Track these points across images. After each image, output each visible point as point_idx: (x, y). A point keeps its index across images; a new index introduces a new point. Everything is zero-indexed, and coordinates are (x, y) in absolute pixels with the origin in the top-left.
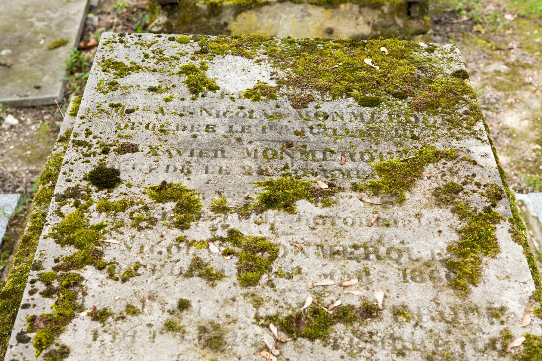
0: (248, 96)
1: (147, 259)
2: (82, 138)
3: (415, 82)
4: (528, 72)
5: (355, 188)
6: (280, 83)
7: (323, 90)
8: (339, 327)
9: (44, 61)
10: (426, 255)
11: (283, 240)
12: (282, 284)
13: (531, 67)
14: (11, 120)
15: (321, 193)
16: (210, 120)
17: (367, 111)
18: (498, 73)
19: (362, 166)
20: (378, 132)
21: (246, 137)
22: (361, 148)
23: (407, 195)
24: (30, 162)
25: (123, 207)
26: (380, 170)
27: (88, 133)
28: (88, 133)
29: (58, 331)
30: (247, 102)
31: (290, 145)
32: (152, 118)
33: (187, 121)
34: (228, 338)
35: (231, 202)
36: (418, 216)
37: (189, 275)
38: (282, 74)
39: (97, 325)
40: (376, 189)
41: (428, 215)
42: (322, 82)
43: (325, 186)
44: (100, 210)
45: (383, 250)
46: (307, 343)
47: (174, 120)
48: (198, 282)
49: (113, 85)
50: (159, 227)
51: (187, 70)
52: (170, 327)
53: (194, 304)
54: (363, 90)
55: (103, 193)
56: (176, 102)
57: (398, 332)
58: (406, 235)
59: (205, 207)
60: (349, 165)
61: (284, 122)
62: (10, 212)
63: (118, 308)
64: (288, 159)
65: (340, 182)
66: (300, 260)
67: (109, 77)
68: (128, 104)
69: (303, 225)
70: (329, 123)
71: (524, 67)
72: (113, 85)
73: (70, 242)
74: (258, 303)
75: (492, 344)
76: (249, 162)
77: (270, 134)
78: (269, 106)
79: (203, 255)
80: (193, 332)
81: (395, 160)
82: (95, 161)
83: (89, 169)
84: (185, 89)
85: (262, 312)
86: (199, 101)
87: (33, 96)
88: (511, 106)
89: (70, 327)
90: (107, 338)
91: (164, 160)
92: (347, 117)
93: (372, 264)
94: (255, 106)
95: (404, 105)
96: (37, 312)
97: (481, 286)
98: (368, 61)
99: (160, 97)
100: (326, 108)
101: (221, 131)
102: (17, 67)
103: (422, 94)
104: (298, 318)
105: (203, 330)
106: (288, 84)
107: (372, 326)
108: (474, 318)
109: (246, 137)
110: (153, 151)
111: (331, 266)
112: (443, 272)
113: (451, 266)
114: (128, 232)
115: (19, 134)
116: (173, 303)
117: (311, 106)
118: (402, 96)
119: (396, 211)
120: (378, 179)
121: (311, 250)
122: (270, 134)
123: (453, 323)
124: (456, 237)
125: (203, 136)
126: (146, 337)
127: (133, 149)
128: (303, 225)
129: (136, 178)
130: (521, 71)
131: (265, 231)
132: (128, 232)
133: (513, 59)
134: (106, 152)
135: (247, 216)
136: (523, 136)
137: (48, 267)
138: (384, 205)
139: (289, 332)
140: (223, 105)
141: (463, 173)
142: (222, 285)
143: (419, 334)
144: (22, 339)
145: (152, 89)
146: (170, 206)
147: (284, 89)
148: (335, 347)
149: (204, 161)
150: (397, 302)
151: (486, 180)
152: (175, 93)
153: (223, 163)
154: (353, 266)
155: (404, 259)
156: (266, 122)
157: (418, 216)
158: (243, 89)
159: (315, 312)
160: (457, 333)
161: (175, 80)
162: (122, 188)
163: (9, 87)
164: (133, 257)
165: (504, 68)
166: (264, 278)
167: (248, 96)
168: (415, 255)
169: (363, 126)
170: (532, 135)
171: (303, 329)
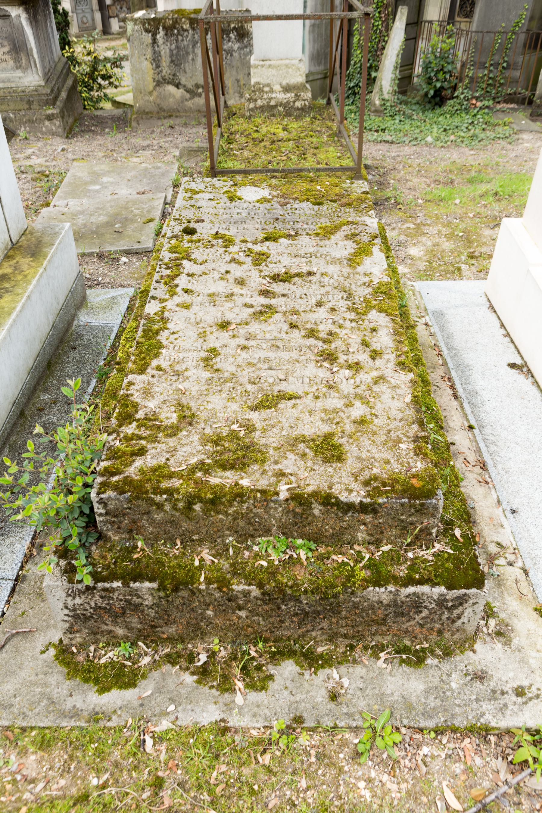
0: (258, 202)
1: (211, 257)
2: (178, 217)
3: (342, 196)
4: (427, 227)
5: (308, 234)
6: (274, 197)
7: (295, 199)
8: (297, 279)
9: (141, 229)
10: (338, 256)
11: (272, 252)
12: (271, 266)
13: (429, 225)
14: (124, 259)
15: (291, 236)
16: (239, 211)
17: (316, 207)
18: (409, 228)
19: (312, 227)
20: (321, 215)
21: (256, 217)
22: (312, 220)
23: (332, 236)
24: (137, 280)
25: (199, 241)
26: (320, 228)
27: (180, 216)
28: (180, 216)
29: (173, 280)
30: (258, 205)
31: (277, 219)
32: (211, 210)
33: (227, 211)
34: (248, 282)
35: (248, 239)
36: (336, 244)
37: (230, 262)
38: (275, 193)
39: (190, 278)
40: (317, 235)
41: (341, 244)
42: (295, 196)
43: (293, 234)
44: (188, 242)
45: (318, 255)
46: (282, 283)
47: (221, 211)
48: (233, 265)
49: (191, 198)
50: (216, 248)
51: (227, 192)
52: (222, 278)
53: (232, 272)
54: (316, 199)
55: (189, 237)
56: (222, 204)
57: (322, 280)
58: (330, 250)
59: (237, 241)
60: (305, 226)
61: (275, 211)
62: (131, 294)
63: (198, 273)
64: (276, 225)
65: (300, 232)
66: (280, 258)
67: (189, 194)
68: (198, 205)
69: (282, 247)
70: (297, 212)
71: (425, 225)
72: (191, 198)
73: (176, 252)
74: (261, 271)
75: (364, 284)
76: (257, 226)
77: (268, 216)
78: (268, 206)
79: (236, 257)
80: (232, 280)
81: (328, 224)
82: (184, 226)
83: (181, 228)
84: (226, 200)
85: (262, 274)
86: (234, 203)
87: (136, 246)
88: (414, 244)
89: (178, 278)
90: (195, 282)
91: (217, 225)
92: (306, 209)
93: (314, 260)
94: (261, 205)
95: (335, 205)
96: (164, 274)
97: (362, 267)
98: (318, 188)
99: (214, 203)
100: (296, 206)
101: (244, 214)
102: (125, 233)
103: (344, 201)
104: (278, 275)
105: (236, 279)
106: (277, 197)
107: (311, 278)
108: (357, 276)
109: (256, 217)
110: (212, 222)
111: (294, 260)
112: (345, 262)
113: (349, 260)
114: (201, 250)
115: (129, 267)
116: (223, 271)
117: (289, 205)
118: (334, 201)
119: (327, 242)
120: (319, 231)
121: (285, 255)
122: (268, 216)
123: (348, 277)
124: (353, 251)
125: (235, 217)
126: (212, 281)
127: (202, 221)
128: (282, 247)
129: (204, 231)
130: (422, 227)
131: (265, 249)
132: (201, 250)
133: (419, 221)
134: (189, 222)
135: (256, 244)
136: (420, 259)
137: (166, 260)
138: (321, 240)
139: (274, 279)
140: (245, 206)
141: (360, 230)
142: (244, 266)
143: (331, 280)
144: (157, 282)
145: (210, 199)
146: (220, 241)
147: (276, 199)
148: (294, 284)
149: (236, 225)
150: (323, 271)
151: (371, 231)
152: (221, 201)
153: (245, 226)
154: (304, 260)
155: (328, 258)
156: (266, 211)
157: (336, 244)
158: (255, 199)
159: (286, 273)
160: (348, 280)
161: (221, 196)
162: (198, 235)
163: (122, 242)
164: (205, 257)
165: (412, 226)
166: (264, 264)
167: (258, 202)
168: (333, 256)
169: (314, 213)
170: (425, 258)
171: (280, 278)
